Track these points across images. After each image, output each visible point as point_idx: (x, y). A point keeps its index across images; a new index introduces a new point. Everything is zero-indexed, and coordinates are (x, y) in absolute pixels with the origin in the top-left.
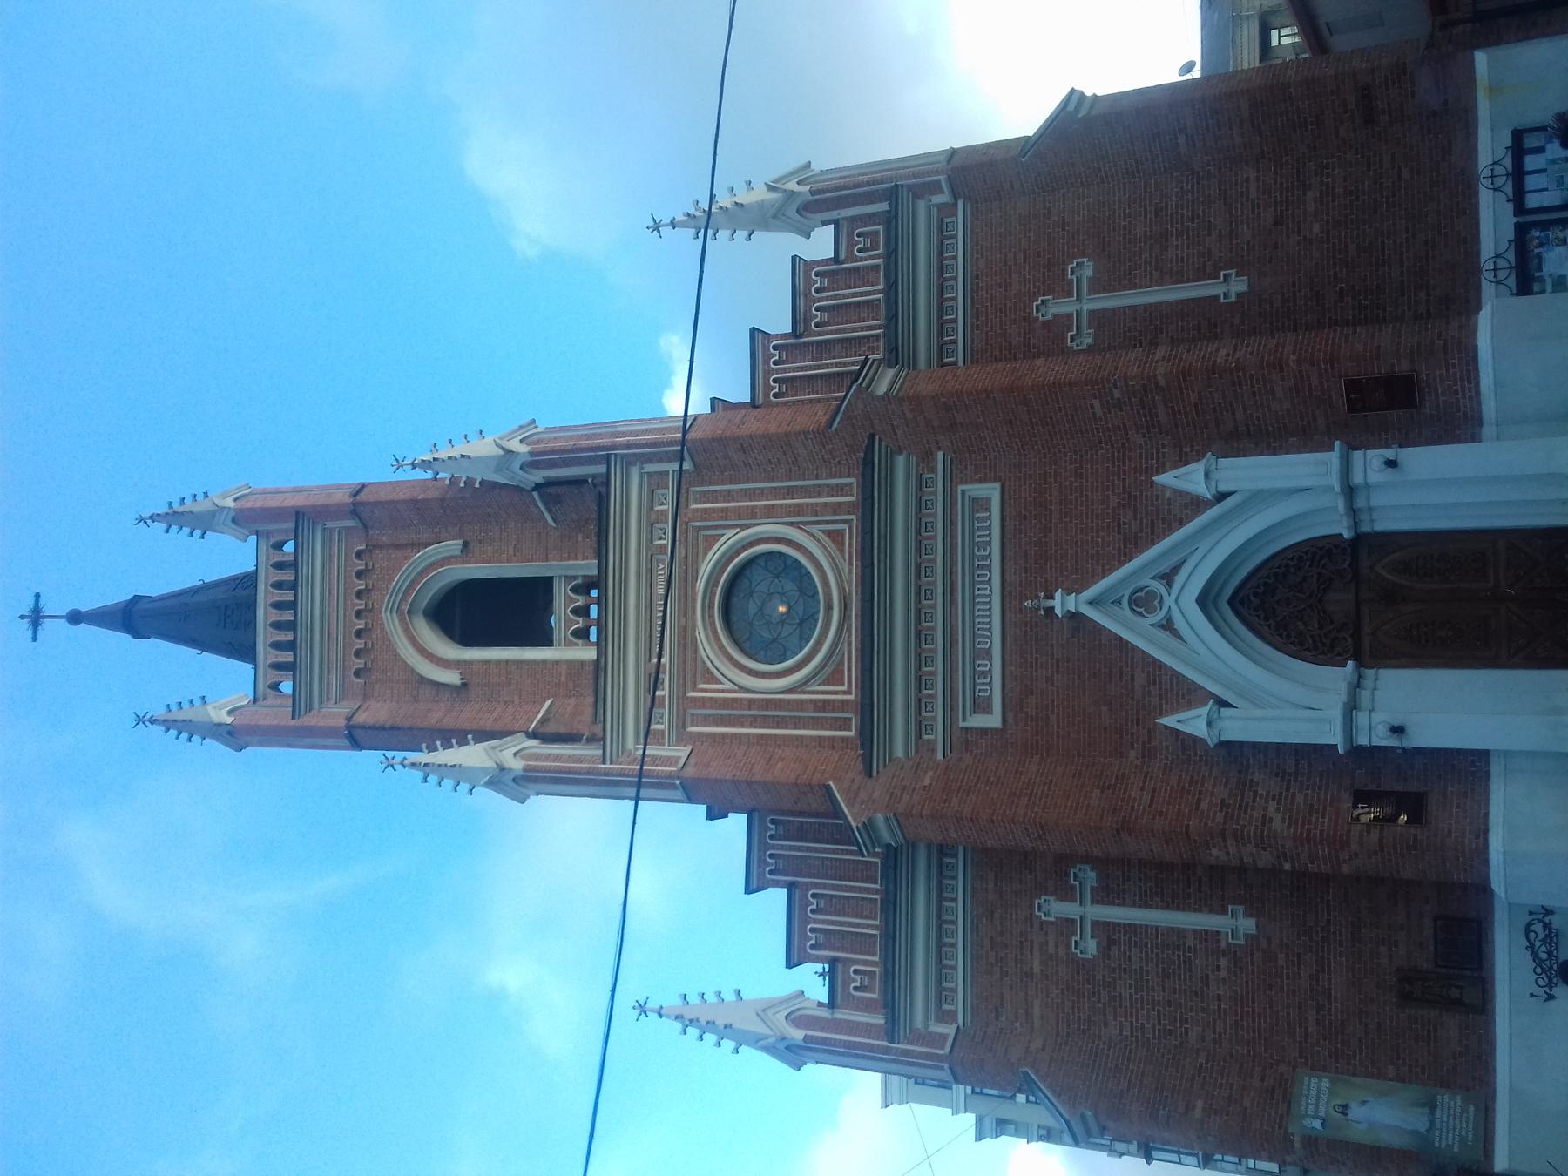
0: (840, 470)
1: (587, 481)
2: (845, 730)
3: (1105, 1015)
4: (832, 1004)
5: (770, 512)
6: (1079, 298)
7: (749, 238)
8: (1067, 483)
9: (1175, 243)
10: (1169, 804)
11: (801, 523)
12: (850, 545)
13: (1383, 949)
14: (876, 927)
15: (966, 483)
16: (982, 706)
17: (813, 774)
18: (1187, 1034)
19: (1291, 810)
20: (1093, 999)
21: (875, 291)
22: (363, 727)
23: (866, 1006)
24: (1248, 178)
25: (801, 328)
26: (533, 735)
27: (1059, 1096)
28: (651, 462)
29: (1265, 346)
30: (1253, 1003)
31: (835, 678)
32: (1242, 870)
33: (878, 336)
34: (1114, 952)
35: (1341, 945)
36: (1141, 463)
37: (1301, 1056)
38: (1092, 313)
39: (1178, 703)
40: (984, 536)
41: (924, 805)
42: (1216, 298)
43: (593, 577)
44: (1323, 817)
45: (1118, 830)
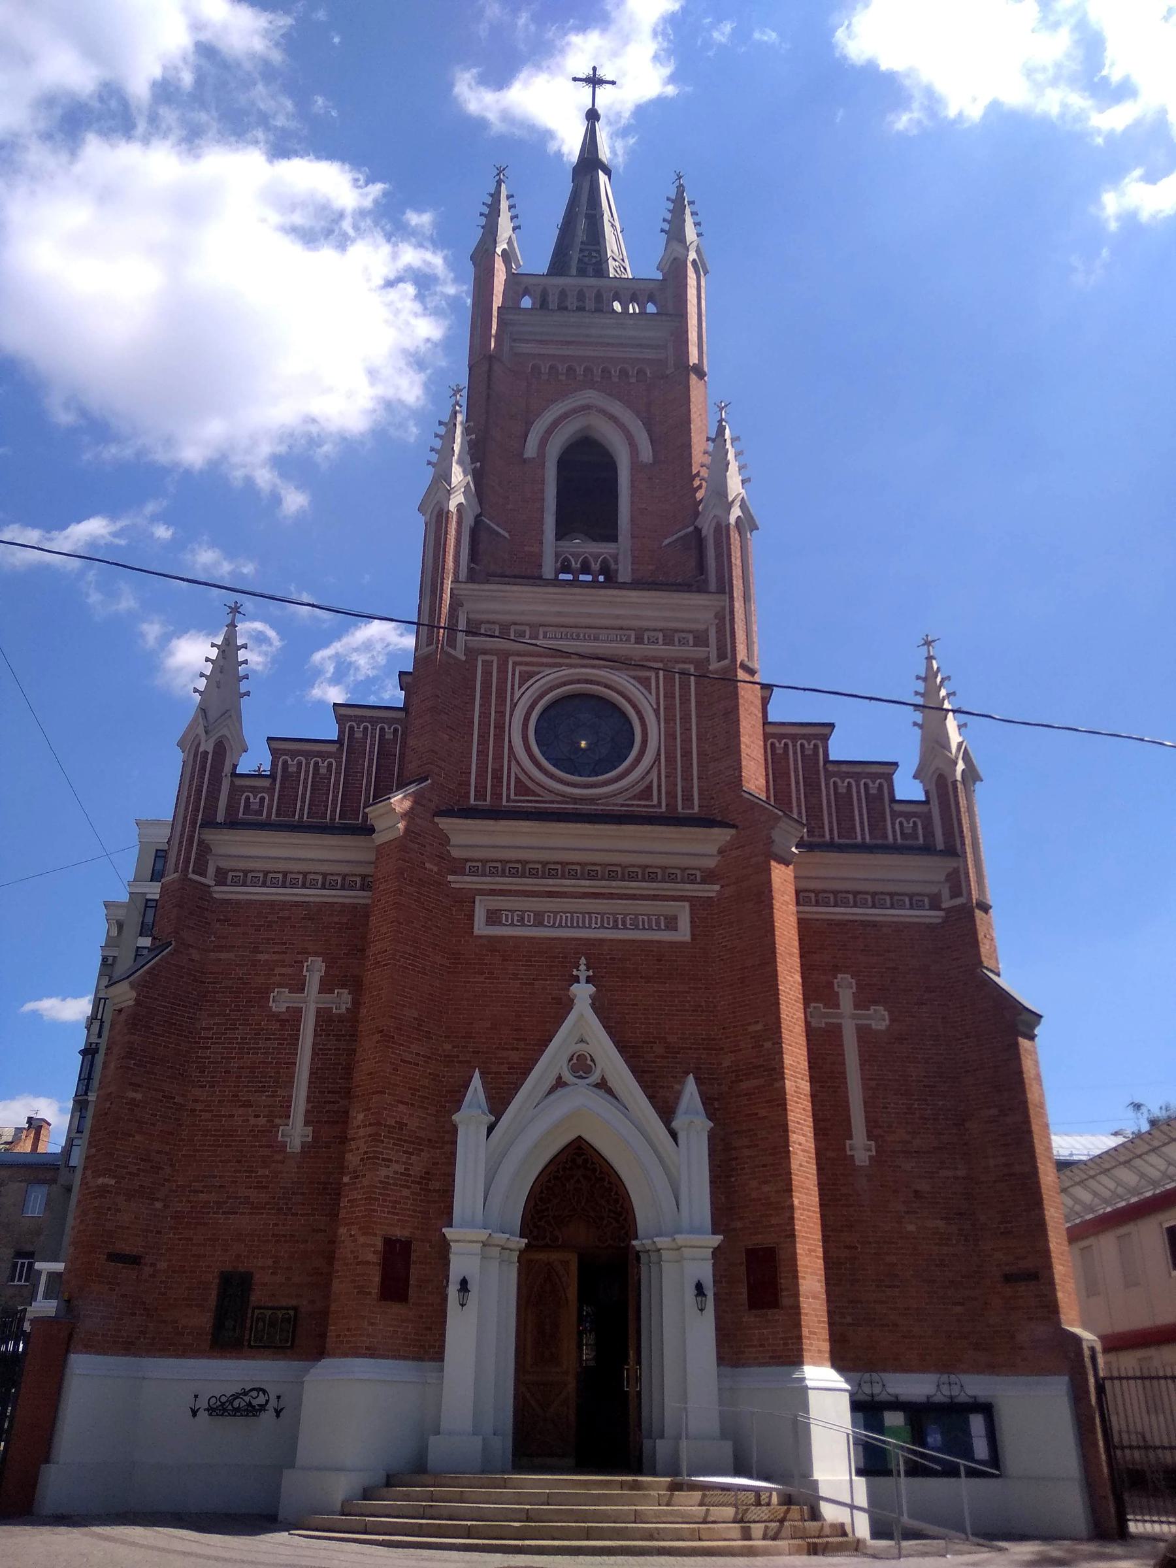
0: (705, 799)
1: (702, 574)
2: (475, 795)
3: (218, 1015)
4: (234, 775)
5: (670, 736)
6: (854, 1017)
7: (915, 724)
8: (689, 998)
9: (900, 1102)
11: (660, 763)
12: (638, 806)
13: (270, 1262)
14: (301, 817)
15: (691, 910)
16: (493, 917)
17: (437, 766)
18: (201, 1087)
19: (394, 1185)
20: (233, 1005)
21: (862, 833)
22: (490, 370)
23: (231, 807)
24: (956, 1169)
25: (830, 767)
26: (478, 518)
27: (147, 972)
28: (717, 632)
29: (807, 1178)
30: (226, 1146)
32: (343, 1139)
33: (823, 836)
34: (275, 1026)
35: (276, 1225)
36: (704, 1064)
37: (178, 1186)
38: (839, 1026)
39: (492, 1088)
40: (643, 922)
43: (617, 578)
44: (389, 1213)
45: (382, 1031)
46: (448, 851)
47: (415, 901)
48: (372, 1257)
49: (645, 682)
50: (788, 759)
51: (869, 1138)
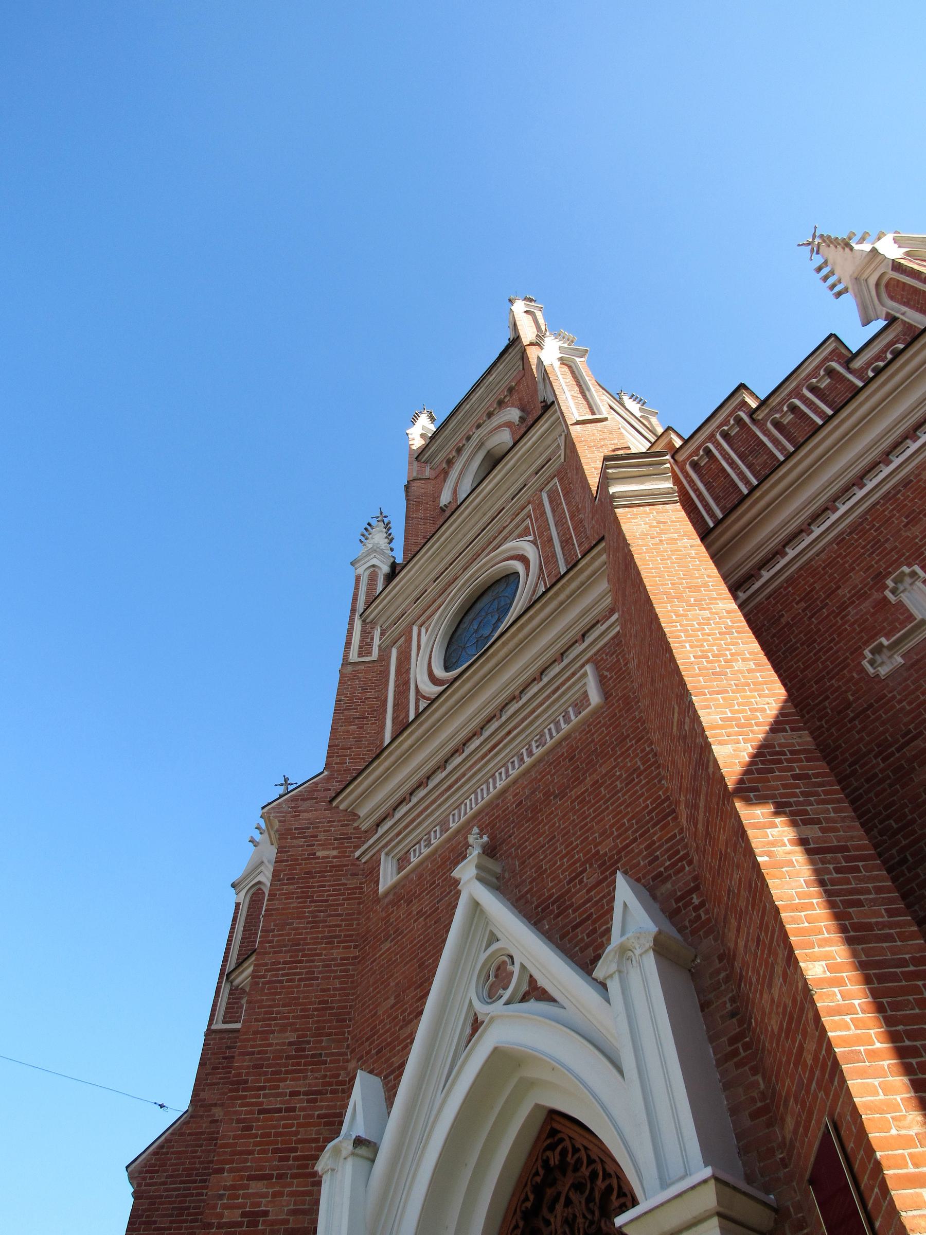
10: (262, 1136)
11: (543, 574)
41: (287, 861)
46: (357, 828)
47: (297, 898)
50: (716, 460)
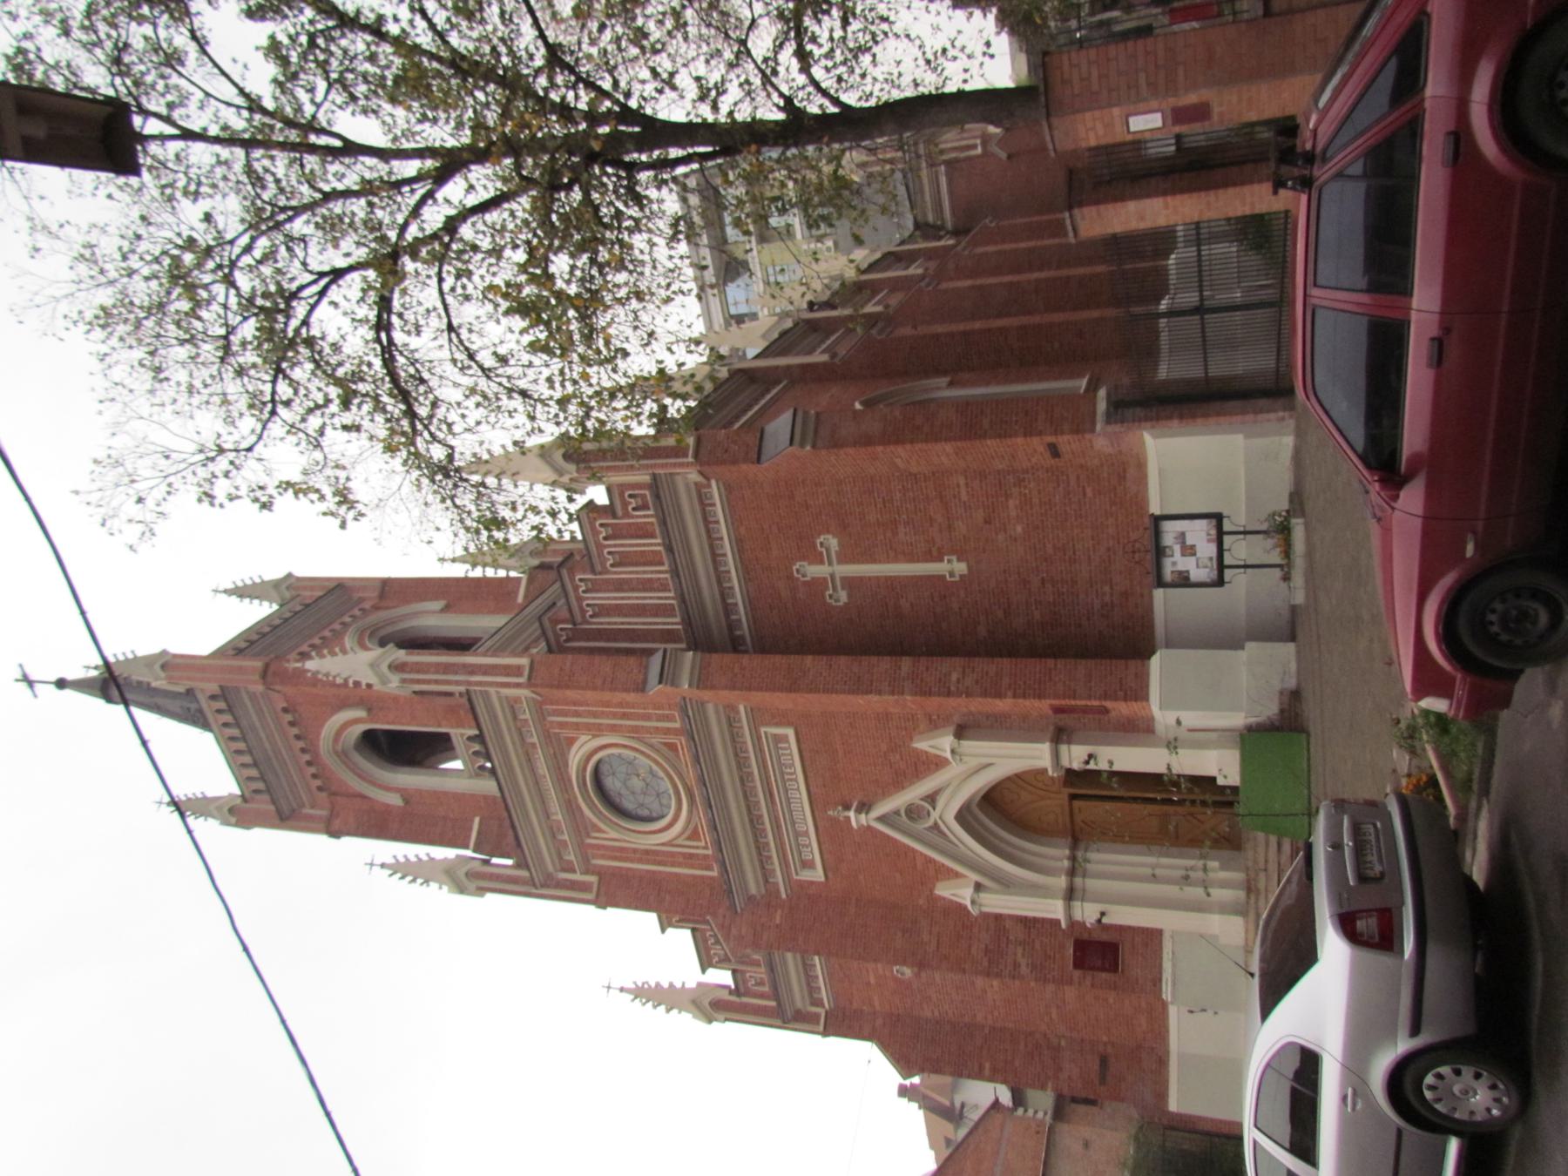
5: (613, 729)
16: (807, 865)
21: (655, 544)
23: (762, 996)
31: (695, 835)
42: (942, 577)
46: (762, 897)
48: (1088, 982)
49: (571, 741)
51: (941, 560)
